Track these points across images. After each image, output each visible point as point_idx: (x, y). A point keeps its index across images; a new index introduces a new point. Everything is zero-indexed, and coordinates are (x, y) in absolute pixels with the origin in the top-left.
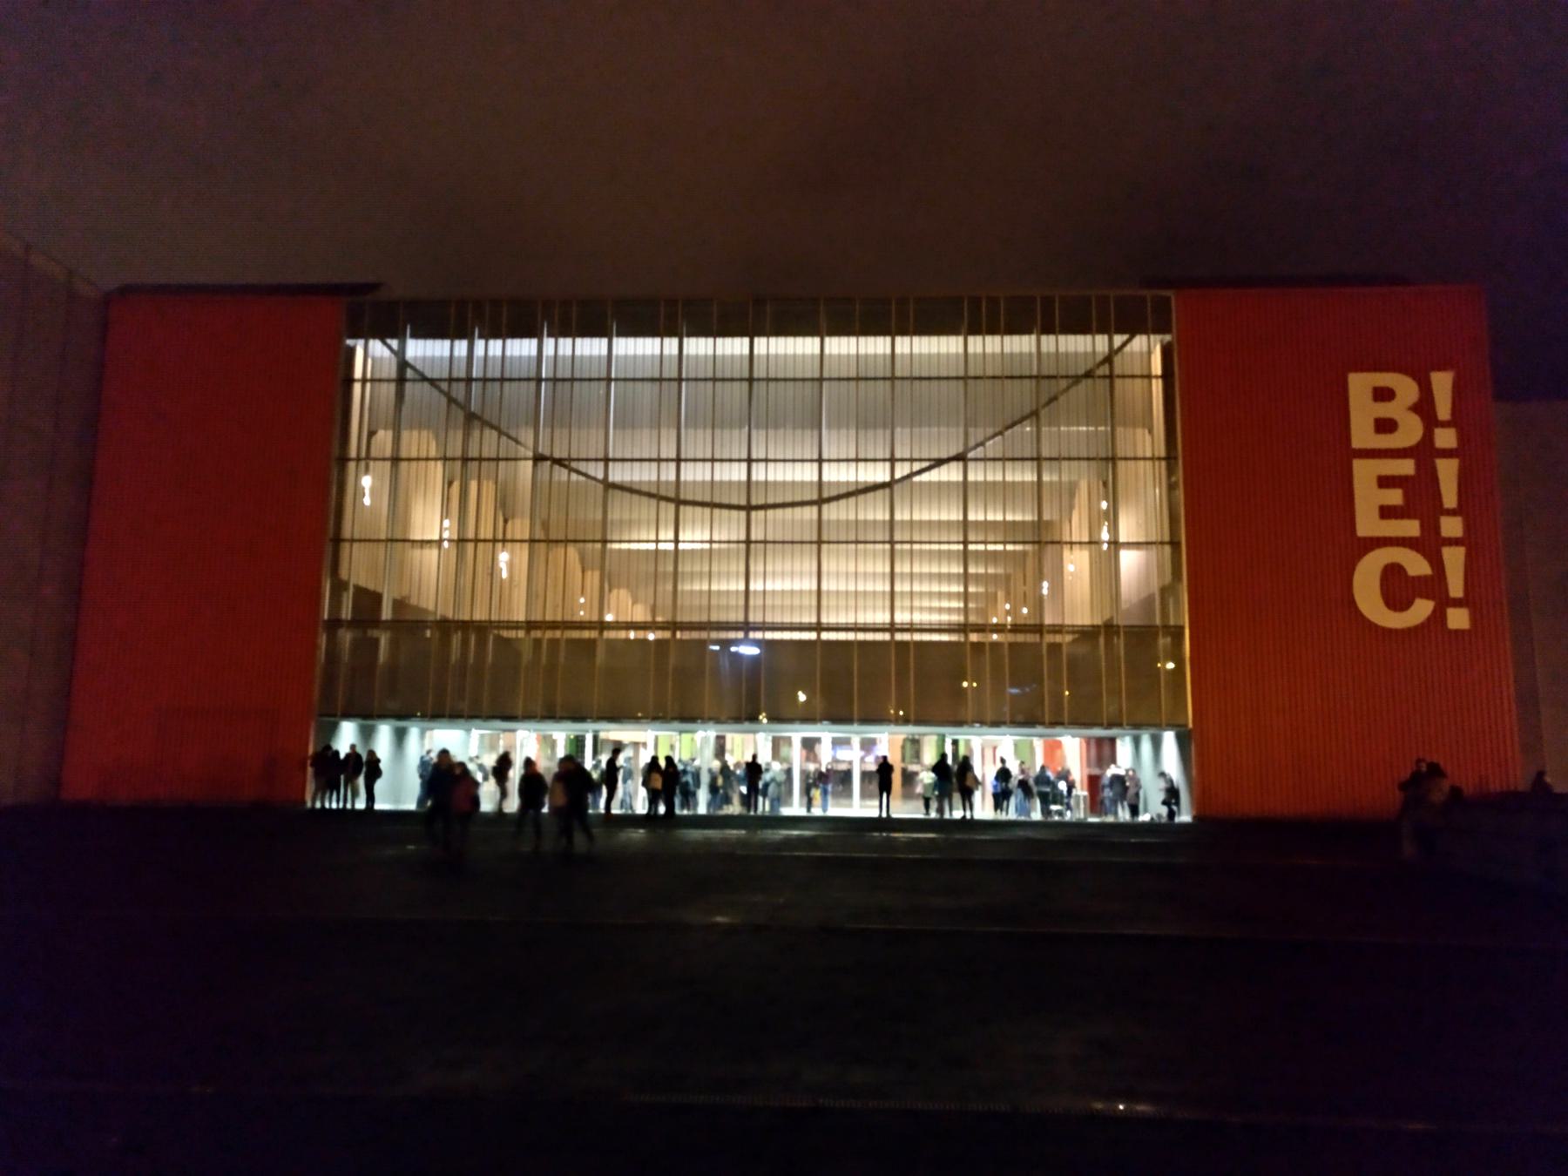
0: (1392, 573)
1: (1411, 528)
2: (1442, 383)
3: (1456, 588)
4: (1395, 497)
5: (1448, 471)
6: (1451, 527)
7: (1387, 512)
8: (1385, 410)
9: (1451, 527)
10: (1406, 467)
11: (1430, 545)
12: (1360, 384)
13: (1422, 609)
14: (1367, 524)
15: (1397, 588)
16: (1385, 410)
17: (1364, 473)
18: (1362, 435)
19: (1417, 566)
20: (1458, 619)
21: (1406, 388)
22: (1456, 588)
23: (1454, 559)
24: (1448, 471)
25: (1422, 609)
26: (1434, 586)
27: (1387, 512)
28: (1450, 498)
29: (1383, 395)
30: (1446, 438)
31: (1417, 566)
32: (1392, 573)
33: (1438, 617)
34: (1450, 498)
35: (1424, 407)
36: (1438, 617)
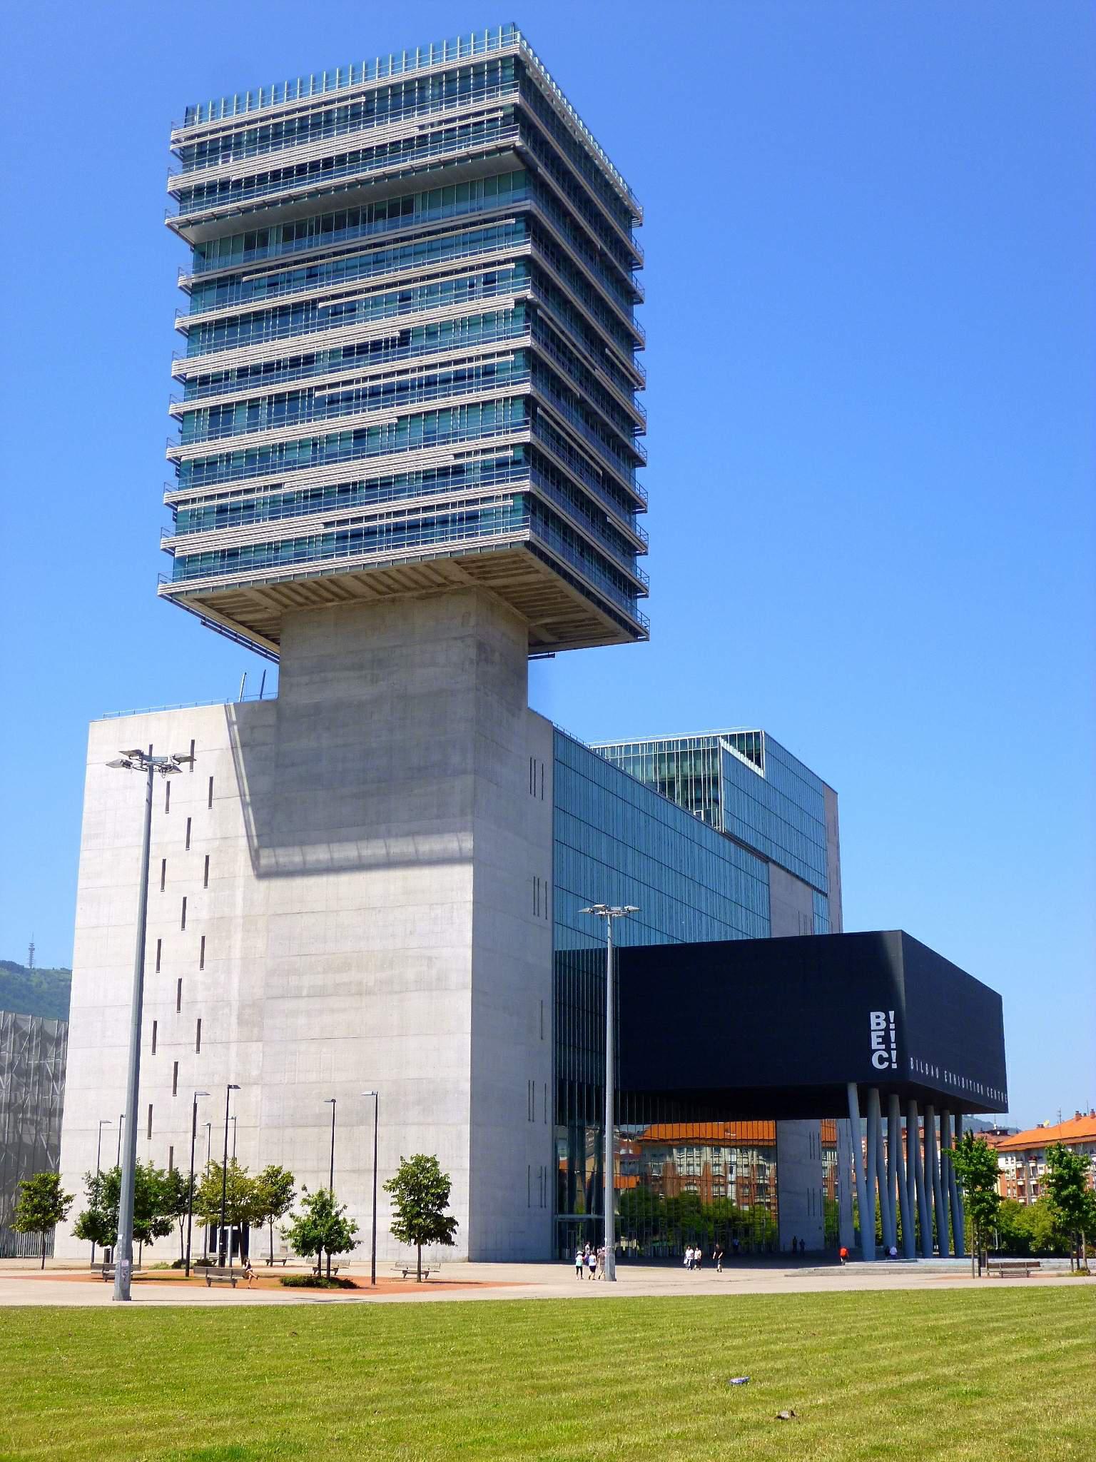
0: (880, 1056)
1: (883, 1047)
2: (892, 1013)
3: (894, 1060)
4: (880, 1040)
5: (893, 1034)
6: (893, 1046)
7: (879, 1043)
8: (878, 1021)
9: (893, 1046)
10: (882, 1033)
11: (888, 1050)
12: (873, 1015)
13: (886, 1064)
14: (874, 1046)
15: (881, 1060)
16: (878, 1021)
17: (874, 1035)
18: (873, 1027)
19: (885, 1055)
20: (894, 1066)
21: (883, 1015)
22: (894, 1060)
23: (894, 1053)
24: (893, 1034)
25: (886, 1064)
26: (889, 1059)
27: (879, 1043)
28: (893, 1040)
29: (878, 1017)
30: (892, 1026)
31: (885, 1055)
32: (880, 1056)
33: (890, 1066)
34: (893, 1040)
35: (887, 1020)
36: (890, 1066)
